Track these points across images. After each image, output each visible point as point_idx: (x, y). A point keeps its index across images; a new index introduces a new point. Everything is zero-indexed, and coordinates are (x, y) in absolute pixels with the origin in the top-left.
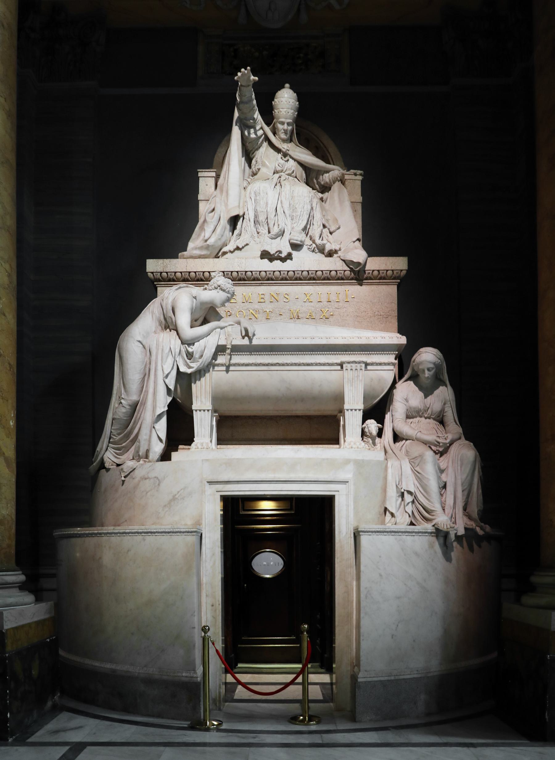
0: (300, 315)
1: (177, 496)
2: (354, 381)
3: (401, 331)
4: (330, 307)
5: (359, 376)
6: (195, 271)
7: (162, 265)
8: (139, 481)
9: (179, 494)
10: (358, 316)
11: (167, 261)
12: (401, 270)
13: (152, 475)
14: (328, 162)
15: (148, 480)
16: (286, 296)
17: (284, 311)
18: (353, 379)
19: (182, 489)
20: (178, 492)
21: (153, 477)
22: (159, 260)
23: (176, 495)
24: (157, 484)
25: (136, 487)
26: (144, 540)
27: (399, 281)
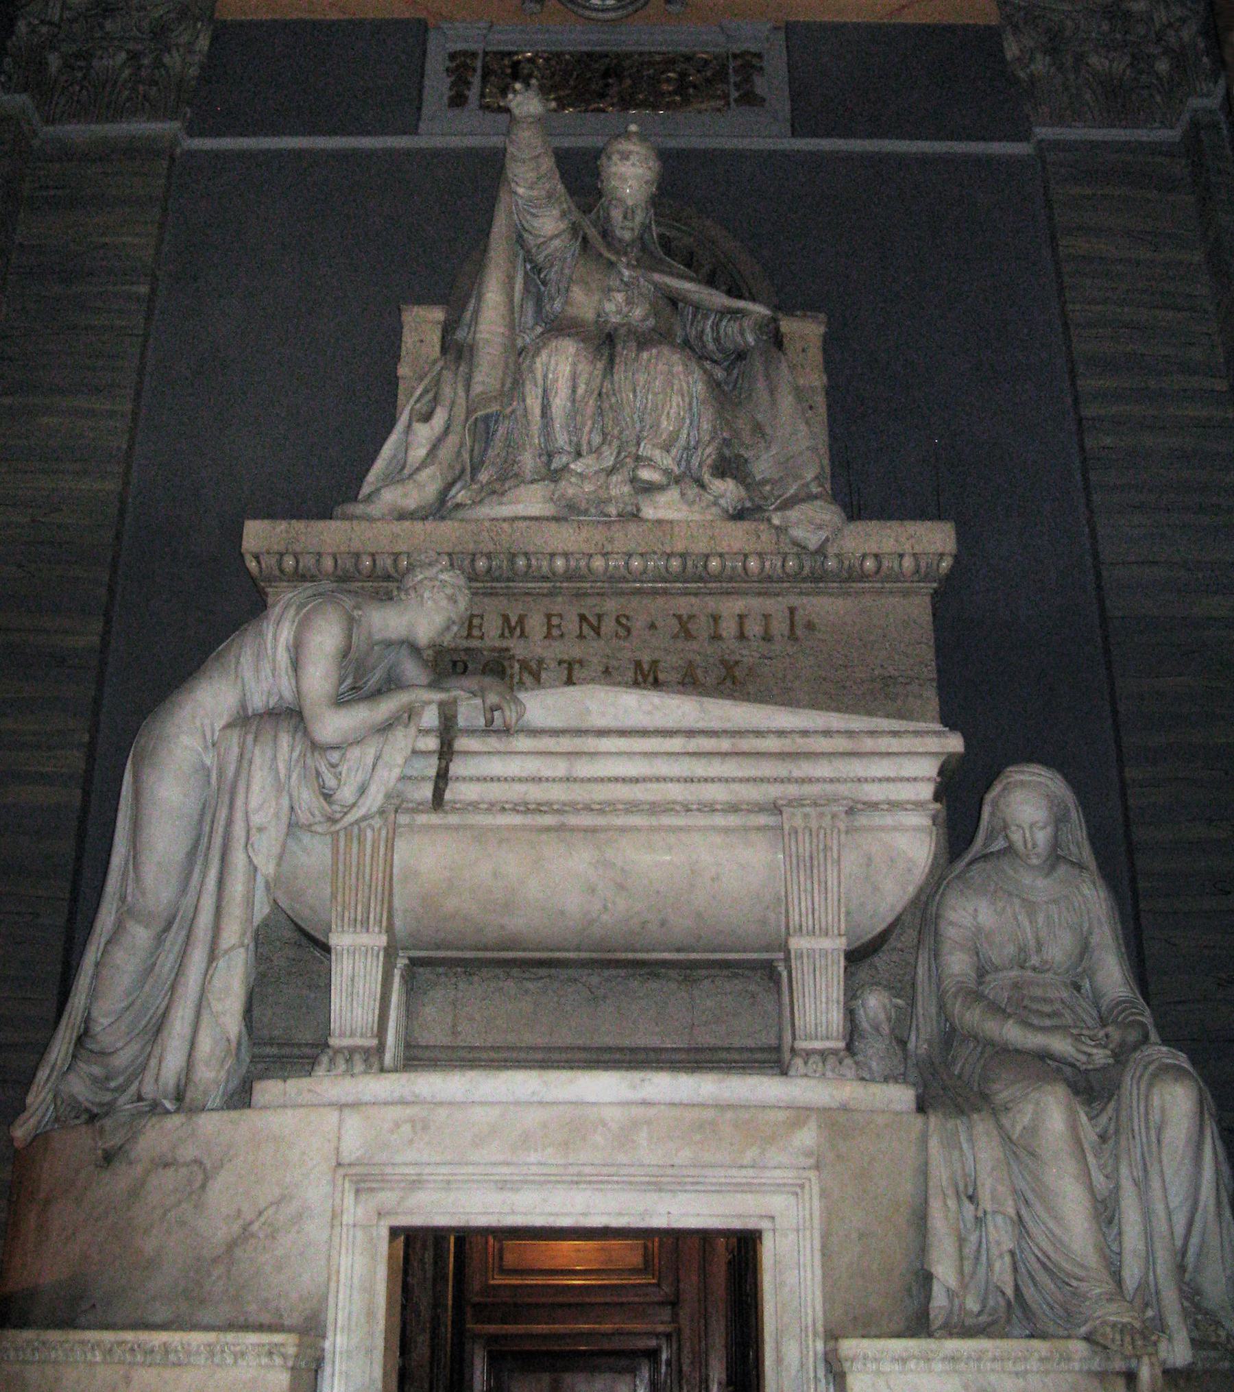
0: (661, 676)
1: (255, 1227)
2: (816, 863)
3: (950, 721)
4: (745, 652)
5: (831, 849)
6: (373, 550)
7: (284, 535)
8: (148, 1172)
9: (262, 1219)
10: (824, 679)
11: (299, 525)
12: (942, 555)
13: (188, 1152)
14: (737, 294)
15: (170, 1172)
16: (624, 621)
17: (615, 663)
18: (811, 858)
19: (272, 1204)
20: (260, 1213)
21: (188, 1159)
22: (278, 522)
23: (251, 1223)
24: (197, 1185)
25: (135, 1193)
26: (128, 1380)
27: (935, 585)
